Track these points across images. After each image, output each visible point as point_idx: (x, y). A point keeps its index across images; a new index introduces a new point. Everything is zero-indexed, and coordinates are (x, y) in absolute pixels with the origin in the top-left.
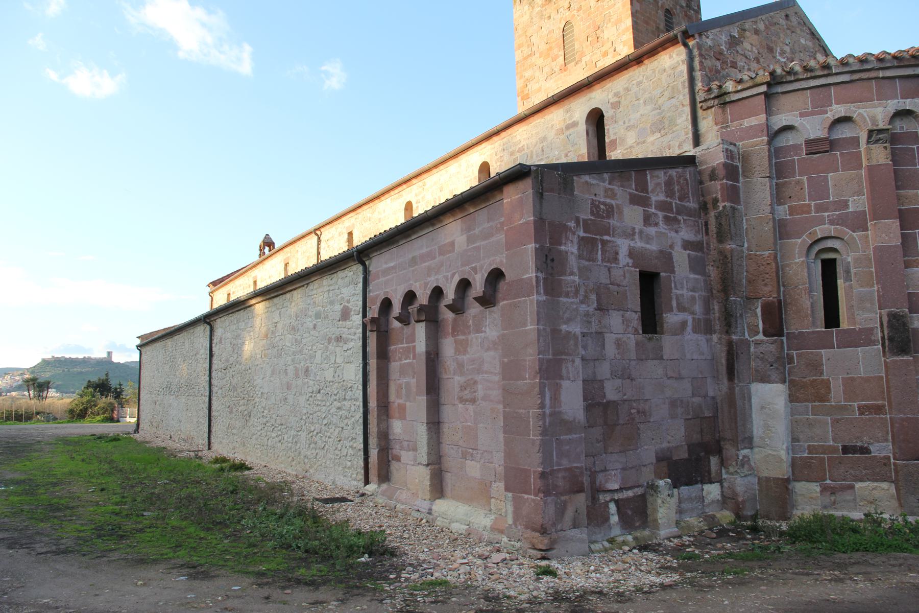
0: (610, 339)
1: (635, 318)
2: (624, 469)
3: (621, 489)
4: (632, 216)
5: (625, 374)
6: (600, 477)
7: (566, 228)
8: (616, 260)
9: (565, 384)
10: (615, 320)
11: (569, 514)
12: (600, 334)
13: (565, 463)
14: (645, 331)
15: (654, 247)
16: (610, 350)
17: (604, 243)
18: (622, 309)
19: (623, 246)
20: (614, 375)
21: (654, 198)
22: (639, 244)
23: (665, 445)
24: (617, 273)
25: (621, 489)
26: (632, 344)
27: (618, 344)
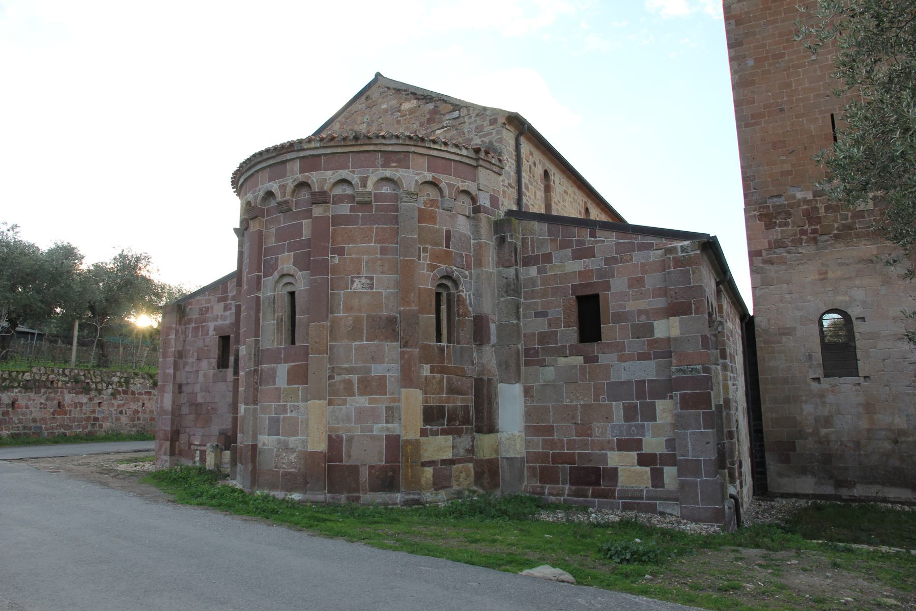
0: (201, 373)
1: (214, 362)
2: (203, 436)
3: (200, 445)
4: (218, 309)
5: (206, 390)
6: (192, 438)
7: (171, 328)
8: (207, 334)
9: (166, 394)
10: (204, 364)
11: (163, 449)
12: (197, 371)
13: (163, 428)
14: (218, 368)
15: (228, 322)
16: (201, 379)
17: (203, 327)
18: (208, 358)
19: (211, 325)
20: (202, 390)
21: (230, 295)
22: (220, 322)
23: (224, 427)
24: (207, 340)
25: (200, 445)
26: (211, 375)
27: (205, 375)
